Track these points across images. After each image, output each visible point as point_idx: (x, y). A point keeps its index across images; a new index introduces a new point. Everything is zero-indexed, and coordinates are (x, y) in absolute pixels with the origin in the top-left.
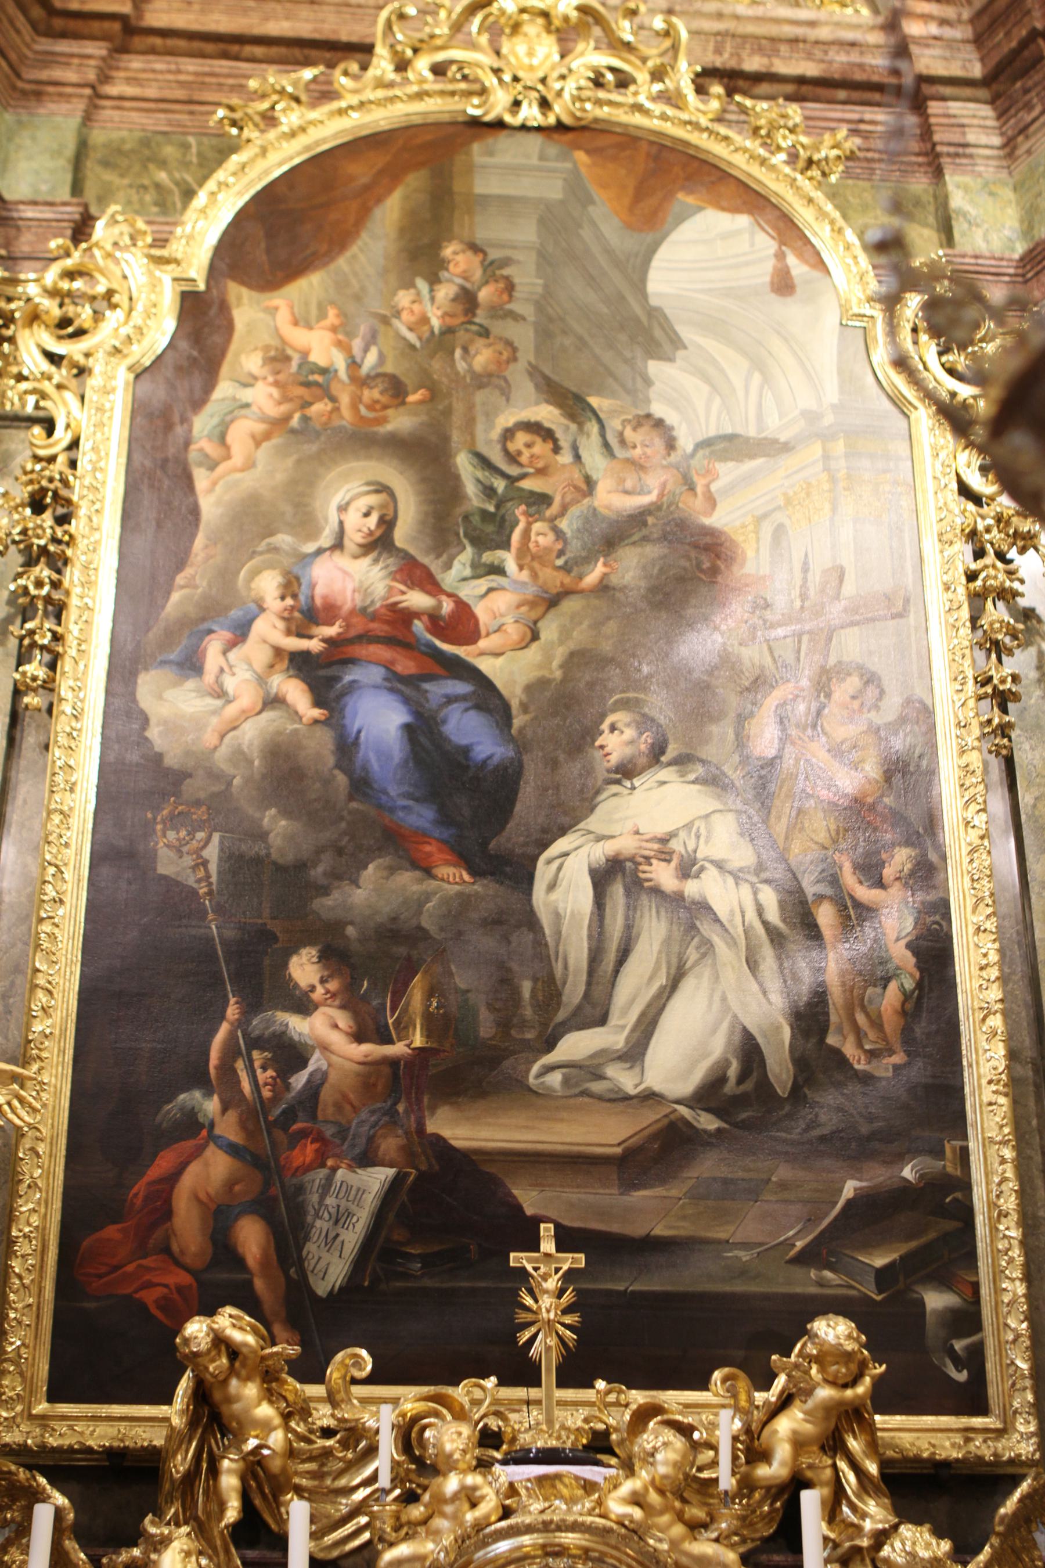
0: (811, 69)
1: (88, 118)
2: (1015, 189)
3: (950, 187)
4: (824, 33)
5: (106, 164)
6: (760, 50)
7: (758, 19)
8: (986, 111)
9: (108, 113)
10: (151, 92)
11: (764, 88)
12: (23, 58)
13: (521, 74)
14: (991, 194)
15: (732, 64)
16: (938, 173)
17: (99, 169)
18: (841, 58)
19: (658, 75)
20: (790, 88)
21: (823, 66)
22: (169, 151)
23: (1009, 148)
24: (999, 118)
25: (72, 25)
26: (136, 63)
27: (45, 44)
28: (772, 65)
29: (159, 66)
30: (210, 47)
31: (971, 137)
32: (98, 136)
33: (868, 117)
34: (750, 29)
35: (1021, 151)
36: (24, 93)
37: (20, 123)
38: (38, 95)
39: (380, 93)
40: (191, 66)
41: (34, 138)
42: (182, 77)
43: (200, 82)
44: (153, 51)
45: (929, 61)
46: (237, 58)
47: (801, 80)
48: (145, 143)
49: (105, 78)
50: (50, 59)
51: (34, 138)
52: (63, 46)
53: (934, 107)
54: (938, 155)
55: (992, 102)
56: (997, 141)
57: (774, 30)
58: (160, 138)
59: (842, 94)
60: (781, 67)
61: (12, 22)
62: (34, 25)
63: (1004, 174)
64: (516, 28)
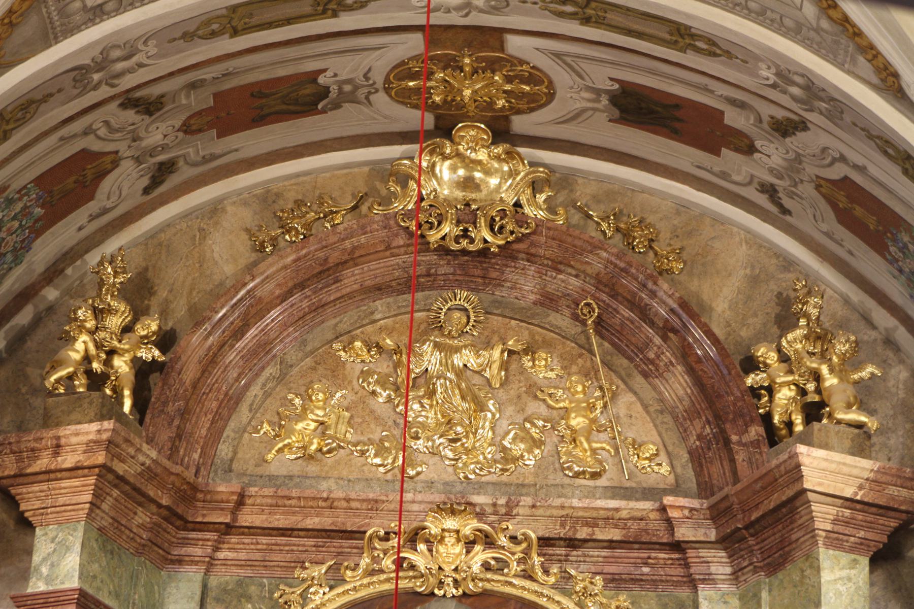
0: (615, 534)
1: (207, 571)
2: (740, 599)
3: (701, 600)
4: (624, 514)
5: (218, 600)
6: (587, 524)
7: (584, 509)
8: (723, 554)
9: (219, 569)
10: (242, 555)
11: (590, 544)
12: (171, 544)
13: (444, 566)
14: (725, 602)
15: (570, 534)
16: (695, 589)
17: (214, 604)
18: (634, 526)
19: (519, 561)
20: (605, 544)
21: (624, 532)
22: (253, 590)
23: (736, 576)
24: (729, 557)
25: (198, 526)
26: (234, 539)
27: (183, 534)
28: (594, 534)
29: (246, 541)
30: (275, 532)
31: (713, 569)
32: (213, 581)
33: (653, 555)
34: (581, 514)
35: (742, 579)
36: (172, 562)
37: (169, 577)
38: (180, 562)
39: (365, 581)
40: (264, 540)
41: (178, 588)
42: (259, 547)
43: (270, 549)
44: (243, 534)
45: (684, 533)
46: (290, 536)
47: (611, 541)
48: (240, 583)
49: (216, 549)
50: (185, 542)
51: (178, 588)
52: (193, 535)
53: (691, 553)
54: (694, 580)
55: (725, 549)
56: (728, 570)
57: (595, 515)
58: (247, 580)
59: (636, 546)
60: (600, 535)
61: (165, 530)
62: (178, 528)
63: (733, 589)
64: (442, 540)
